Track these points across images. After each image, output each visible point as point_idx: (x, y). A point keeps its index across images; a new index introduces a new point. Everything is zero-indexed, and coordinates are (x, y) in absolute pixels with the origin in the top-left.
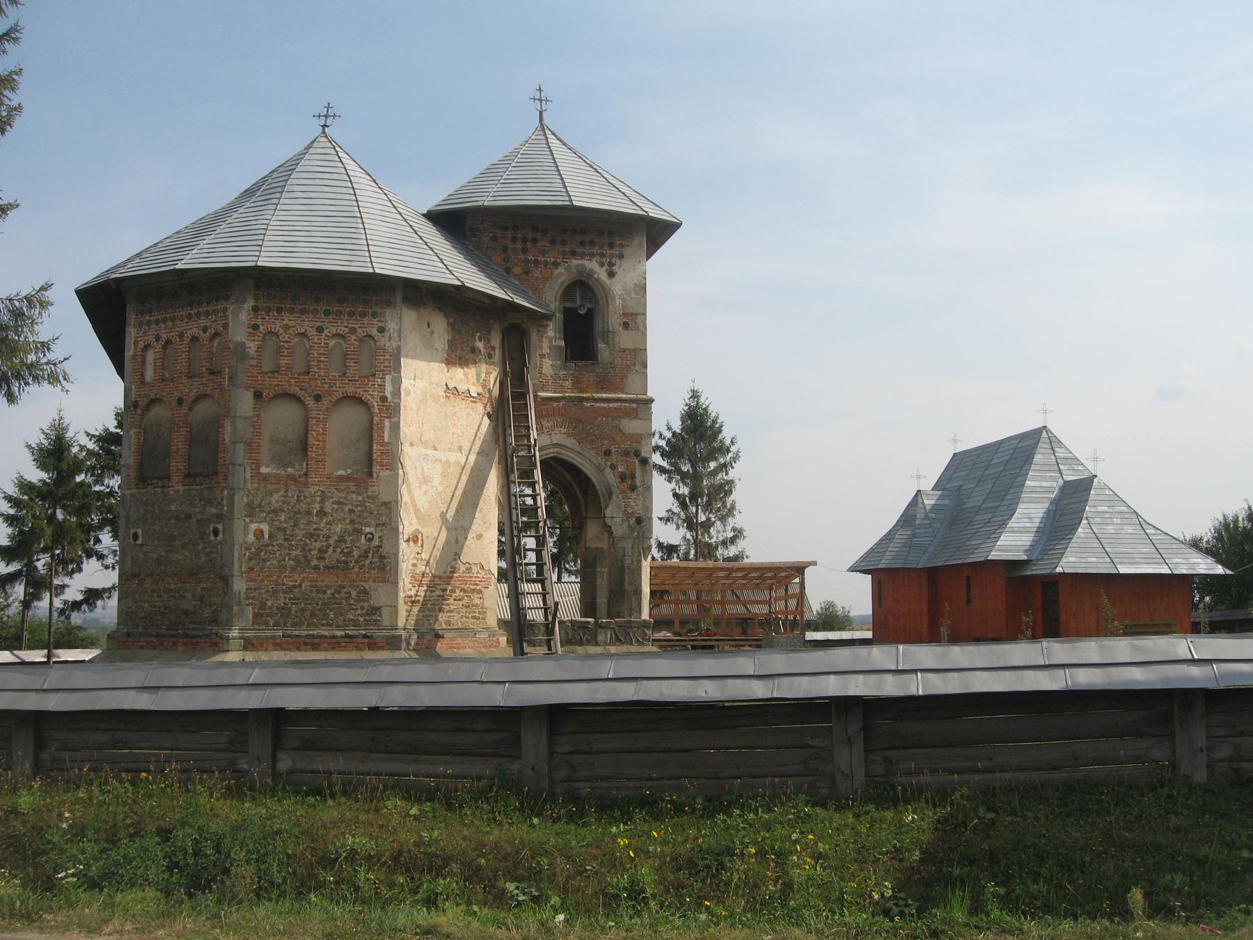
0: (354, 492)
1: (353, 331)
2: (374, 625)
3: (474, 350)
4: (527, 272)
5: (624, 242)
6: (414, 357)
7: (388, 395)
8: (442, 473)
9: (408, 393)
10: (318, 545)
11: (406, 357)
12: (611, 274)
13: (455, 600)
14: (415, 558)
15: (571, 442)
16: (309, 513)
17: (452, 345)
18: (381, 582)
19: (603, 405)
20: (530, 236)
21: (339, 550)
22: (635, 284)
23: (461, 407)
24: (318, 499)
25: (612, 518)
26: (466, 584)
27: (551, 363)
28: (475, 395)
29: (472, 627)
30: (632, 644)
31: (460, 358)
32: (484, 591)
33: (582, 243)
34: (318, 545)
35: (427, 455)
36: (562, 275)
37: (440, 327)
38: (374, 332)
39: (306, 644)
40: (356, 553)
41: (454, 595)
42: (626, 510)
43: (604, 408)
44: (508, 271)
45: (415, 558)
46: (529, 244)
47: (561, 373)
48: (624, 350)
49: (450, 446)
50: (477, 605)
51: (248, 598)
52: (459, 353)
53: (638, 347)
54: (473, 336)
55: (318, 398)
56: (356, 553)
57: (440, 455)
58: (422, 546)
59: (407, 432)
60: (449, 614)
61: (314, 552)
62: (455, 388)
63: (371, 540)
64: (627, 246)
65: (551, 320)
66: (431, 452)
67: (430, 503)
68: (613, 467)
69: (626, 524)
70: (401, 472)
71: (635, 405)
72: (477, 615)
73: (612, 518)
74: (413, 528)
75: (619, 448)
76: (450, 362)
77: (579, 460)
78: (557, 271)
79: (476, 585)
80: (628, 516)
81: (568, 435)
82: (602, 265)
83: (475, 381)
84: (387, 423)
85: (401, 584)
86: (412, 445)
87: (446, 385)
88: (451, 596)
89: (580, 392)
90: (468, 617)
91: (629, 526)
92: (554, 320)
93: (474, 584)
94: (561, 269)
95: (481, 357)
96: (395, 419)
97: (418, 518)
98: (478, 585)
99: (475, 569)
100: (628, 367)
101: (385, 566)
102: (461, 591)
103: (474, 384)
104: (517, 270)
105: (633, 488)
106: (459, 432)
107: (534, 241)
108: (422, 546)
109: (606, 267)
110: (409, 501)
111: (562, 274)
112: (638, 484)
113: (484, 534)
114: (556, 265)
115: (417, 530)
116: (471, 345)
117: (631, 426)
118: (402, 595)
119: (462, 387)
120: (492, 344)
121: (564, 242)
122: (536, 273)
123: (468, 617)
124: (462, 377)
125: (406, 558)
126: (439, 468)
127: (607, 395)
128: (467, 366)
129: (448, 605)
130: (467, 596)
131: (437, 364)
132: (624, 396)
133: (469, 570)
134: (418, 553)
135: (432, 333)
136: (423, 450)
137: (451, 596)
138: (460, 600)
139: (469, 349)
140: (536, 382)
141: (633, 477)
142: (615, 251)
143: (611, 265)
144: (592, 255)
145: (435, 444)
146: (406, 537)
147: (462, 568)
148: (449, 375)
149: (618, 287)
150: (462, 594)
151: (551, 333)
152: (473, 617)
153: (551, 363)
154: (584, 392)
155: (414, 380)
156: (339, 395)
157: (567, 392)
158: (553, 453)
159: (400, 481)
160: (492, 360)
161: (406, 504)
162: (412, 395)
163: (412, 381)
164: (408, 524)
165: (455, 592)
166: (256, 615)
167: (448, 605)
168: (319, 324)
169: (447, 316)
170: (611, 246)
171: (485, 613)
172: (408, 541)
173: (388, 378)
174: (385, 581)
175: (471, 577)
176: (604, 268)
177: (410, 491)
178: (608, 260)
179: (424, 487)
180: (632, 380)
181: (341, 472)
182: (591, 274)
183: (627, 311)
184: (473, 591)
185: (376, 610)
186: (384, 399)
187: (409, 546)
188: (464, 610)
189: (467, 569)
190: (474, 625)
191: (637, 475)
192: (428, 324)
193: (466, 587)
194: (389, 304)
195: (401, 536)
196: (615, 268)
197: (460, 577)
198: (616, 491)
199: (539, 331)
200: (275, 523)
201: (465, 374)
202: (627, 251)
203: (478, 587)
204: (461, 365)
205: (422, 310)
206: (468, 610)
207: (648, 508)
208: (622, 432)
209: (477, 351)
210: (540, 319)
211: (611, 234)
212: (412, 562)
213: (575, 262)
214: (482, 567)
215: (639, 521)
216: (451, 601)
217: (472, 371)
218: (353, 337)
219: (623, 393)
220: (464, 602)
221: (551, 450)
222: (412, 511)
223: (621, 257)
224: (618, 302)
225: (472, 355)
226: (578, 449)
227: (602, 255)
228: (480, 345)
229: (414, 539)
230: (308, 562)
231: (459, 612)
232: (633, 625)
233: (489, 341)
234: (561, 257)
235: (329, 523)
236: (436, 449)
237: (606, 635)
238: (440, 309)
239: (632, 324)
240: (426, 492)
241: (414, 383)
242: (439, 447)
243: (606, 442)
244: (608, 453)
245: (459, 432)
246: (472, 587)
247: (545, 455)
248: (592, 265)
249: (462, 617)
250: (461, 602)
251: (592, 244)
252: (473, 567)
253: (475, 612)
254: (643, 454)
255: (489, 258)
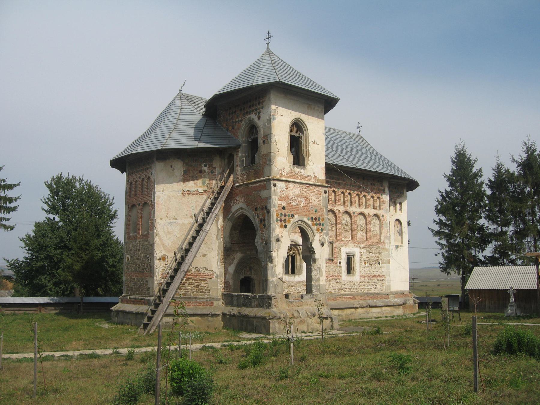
0: (145, 241)
1: (146, 175)
2: (149, 294)
3: (201, 172)
4: (233, 128)
5: (264, 100)
6: (162, 183)
7: (152, 200)
8: (180, 229)
9: (159, 197)
10: (138, 262)
11: (158, 183)
12: (259, 118)
13: (188, 284)
14: (164, 267)
15: (244, 206)
16: (137, 250)
17: (185, 172)
18: (150, 277)
19: (255, 185)
20: (234, 110)
21: (142, 264)
22: (267, 120)
23: (192, 198)
24: (138, 244)
25: (258, 242)
26: (197, 277)
27: (240, 168)
28: (202, 191)
29: (201, 296)
30: (264, 308)
31: (192, 177)
32: (208, 280)
33: (250, 107)
34: (138, 262)
35: (170, 222)
36: (243, 125)
37: (179, 167)
38: (150, 175)
39: (132, 301)
40: (145, 266)
41: (188, 282)
42: (262, 238)
43: (254, 187)
44: (227, 130)
45: (164, 267)
46: (234, 114)
47: (243, 173)
48: (263, 155)
49: (185, 216)
50: (203, 287)
51: (126, 284)
52: (191, 174)
53: (268, 152)
54: (200, 165)
55: (139, 204)
56: (145, 266)
57: (180, 221)
58: (168, 261)
59: (159, 214)
60: (185, 291)
61: (138, 265)
62: (189, 190)
63: (148, 260)
64: (265, 101)
65: (239, 148)
66: (172, 221)
67: (172, 242)
68: (258, 216)
69: (262, 246)
70: (155, 231)
71: (265, 183)
72: (204, 291)
73: (258, 242)
74: (162, 254)
75: (260, 206)
76: (184, 181)
77: (249, 214)
78: (242, 124)
79: (203, 277)
80: (262, 240)
81: (244, 203)
82: (256, 114)
83: (201, 185)
84: (152, 212)
85: (155, 278)
86: (161, 219)
87: (183, 190)
88: (187, 282)
89: (249, 181)
90: (198, 292)
91: (263, 246)
92: (241, 148)
93: (201, 277)
94: (243, 122)
95: (205, 174)
96: (154, 210)
97: (165, 250)
98: (205, 277)
99: (202, 271)
100: (265, 163)
101: (149, 270)
102: (193, 280)
103: (201, 187)
104: (230, 128)
105: (265, 226)
106: (191, 210)
107: (235, 112)
108: (168, 261)
109: (258, 115)
110: (159, 243)
111: (243, 124)
112: (266, 224)
113: (208, 254)
114: (241, 121)
115: (165, 255)
116: (199, 169)
117: (264, 194)
118: (156, 282)
119: (192, 190)
120: (214, 166)
121: (244, 109)
122: (236, 127)
123: (198, 292)
124: (193, 185)
125: (158, 267)
126: (178, 227)
127: (262, 179)
128: (197, 180)
129: (185, 286)
130: (197, 283)
131: (176, 184)
132: (264, 178)
133: (198, 270)
134: (165, 265)
135: (174, 169)
136: (168, 221)
137: (187, 282)
138: (191, 284)
139: (198, 172)
140: (235, 179)
141: (264, 220)
142: (261, 106)
143: (259, 113)
144: (253, 111)
145: (175, 217)
146: (158, 258)
147: (194, 270)
148: (185, 185)
149: (260, 124)
150: (193, 281)
151: (240, 155)
152: (200, 292)
153: (240, 168)
154: (250, 180)
155: (163, 191)
156: (143, 202)
157: (245, 182)
158: (240, 212)
159: (155, 235)
160: (214, 173)
161: (158, 244)
162: (161, 198)
163: (161, 192)
164: (158, 252)
165: (189, 281)
166: (127, 290)
167: (185, 286)
168: (140, 175)
169: (182, 160)
170: (259, 103)
171: (210, 290)
172: (159, 259)
173: (152, 192)
174: (151, 277)
175: (200, 274)
176: (257, 116)
177: (160, 239)
178: (258, 111)
179: (168, 236)
180: (266, 170)
181: (145, 233)
182: (253, 119)
183: (264, 135)
184: (201, 280)
185: (149, 288)
186: (152, 201)
187: (160, 262)
188: (195, 289)
189: (197, 270)
190: (201, 295)
191: (266, 219)
192: (171, 166)
193: (196, 279)
194: (153, 162)
195: (155, 258)
196: (261, 114)
197: (192, 274)
198: (259, 228)
199: (236, 154)
200: (131, 254)
201: (194, 183)
202: (264, 104)
203: (205, 278)
204: (193, 180)
205: (167, 161)
206: (198, 289)
207: (269, 236)
208: (261, 197)
209: (203, 172)
210: (236, 148)
211: (259, 98)
212: (162, 268)
213: (248, 117)
214: (207, 269)
215: (266, 244)
216: (187, 284)
217: (200, 182)
218: (146, 178)
219: (263, 177)
220: (195, 285)
221: (240, 211)
222: (161, 247)
223: (262, 108)
224: (261, 131)
225: (200, 174)
226: (247, 209)
227: (256, 110)
228: (206, 169)
229: (163, 258)
230: (136, 269)
231: (191, 290)
232: (265, 298)
233: (212, 165)
234: (243, 116)
235: (140, 254)
236: (176, 219)
237: (255, 303)
238: (178, 158)
239: (266, 140)
240: (170, 238)
241: (162, 193)
242: (178, 218)
243: (256, 204)
244: (256, 209)
245: (191, 210)
246: (200, 278)
247: (239, 213)
248: (253, 116)
249: (193, 292)
250: (193, 285)
251: (253, 105)
252: (201, 269)
253: (202, 290)
254: (268, 208)
255: (222, 126)
